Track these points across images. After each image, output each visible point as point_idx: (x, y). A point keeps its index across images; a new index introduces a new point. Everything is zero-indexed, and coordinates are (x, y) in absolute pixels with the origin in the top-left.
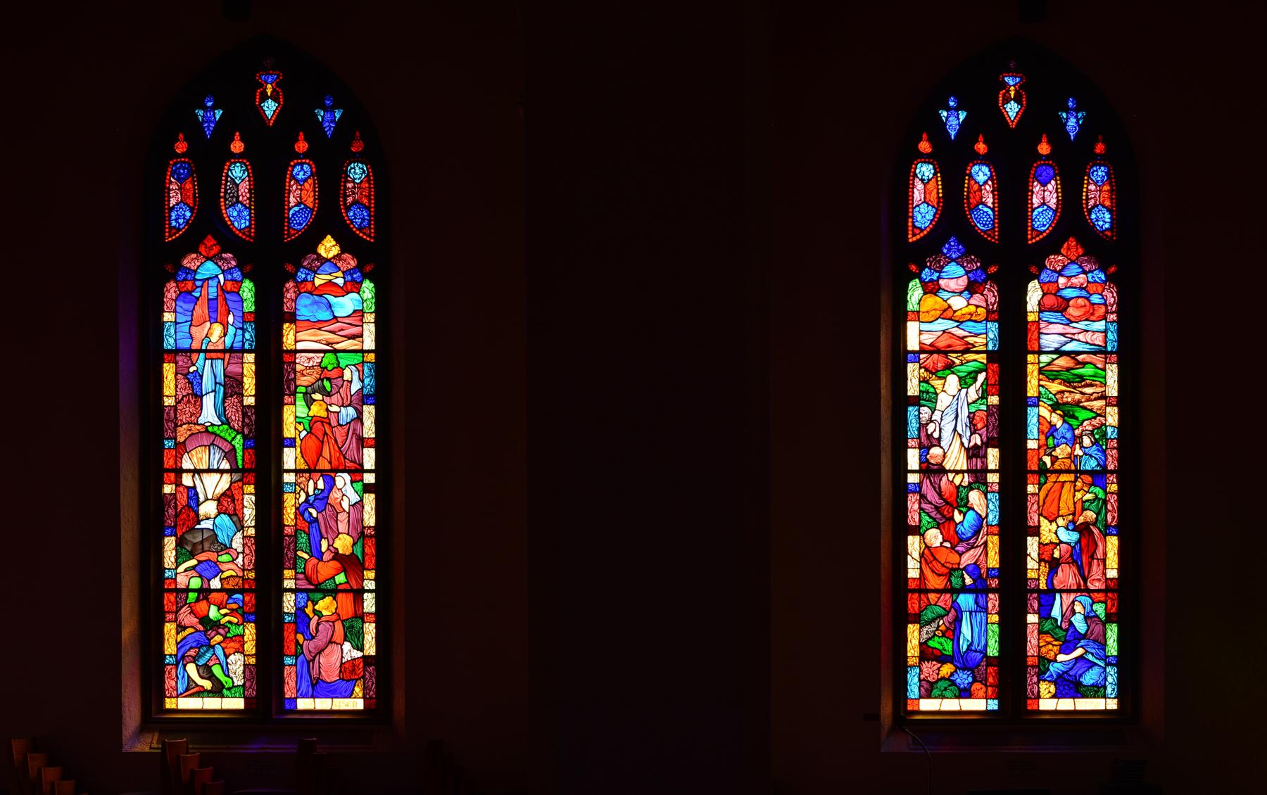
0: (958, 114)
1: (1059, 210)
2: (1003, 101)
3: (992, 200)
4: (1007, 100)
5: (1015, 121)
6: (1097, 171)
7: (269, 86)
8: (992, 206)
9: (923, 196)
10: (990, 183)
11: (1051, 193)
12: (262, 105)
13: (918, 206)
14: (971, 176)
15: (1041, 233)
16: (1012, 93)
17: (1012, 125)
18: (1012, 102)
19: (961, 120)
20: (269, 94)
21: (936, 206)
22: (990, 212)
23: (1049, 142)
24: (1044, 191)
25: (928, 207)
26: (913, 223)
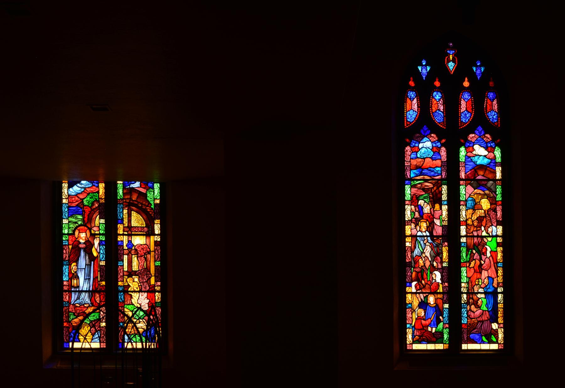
0: (427, 68)
2: (447, 61)
3: (442, 108)
4: (449, 61)
5: (453, 71)
8: (442, 111)
9: (411, 106)
10: (441, 100)
14: (433, 97)
16: (451, 58)
17: (451, 72)
18: (451, 62)
19: (428, 71)
21: (417, 111)
22: (442, 114)
23: (468, 81)
25: (413, 112)
26: (407, 119)
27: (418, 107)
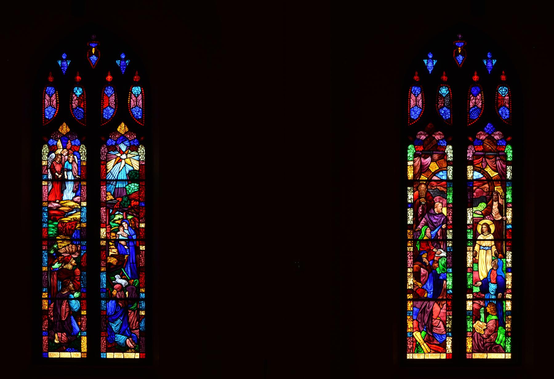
0: (433, 61)
1: (483, 109)
6: (502, 89)
7: (94, 49)
9: (415, 102)
11: (479, 100)
12: (90, 58)
13: (413, 107)
15: (475, 120)
19: (434, 65)
20: (93, 53)
23: (477, 75)
24: (476, 99)
25: (418, 108)
27: (422, 103)
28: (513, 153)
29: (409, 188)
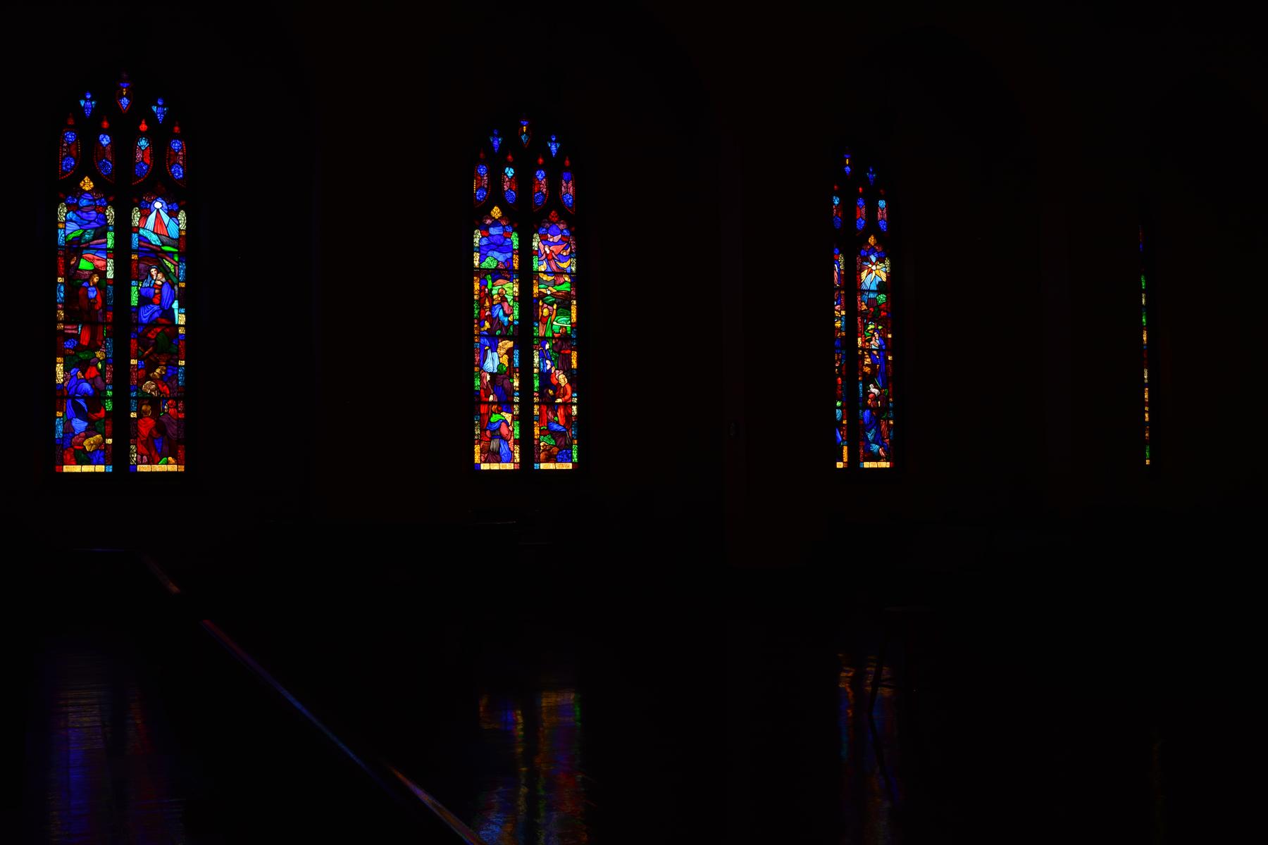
28: (519, 241)
29: (475, 278)
